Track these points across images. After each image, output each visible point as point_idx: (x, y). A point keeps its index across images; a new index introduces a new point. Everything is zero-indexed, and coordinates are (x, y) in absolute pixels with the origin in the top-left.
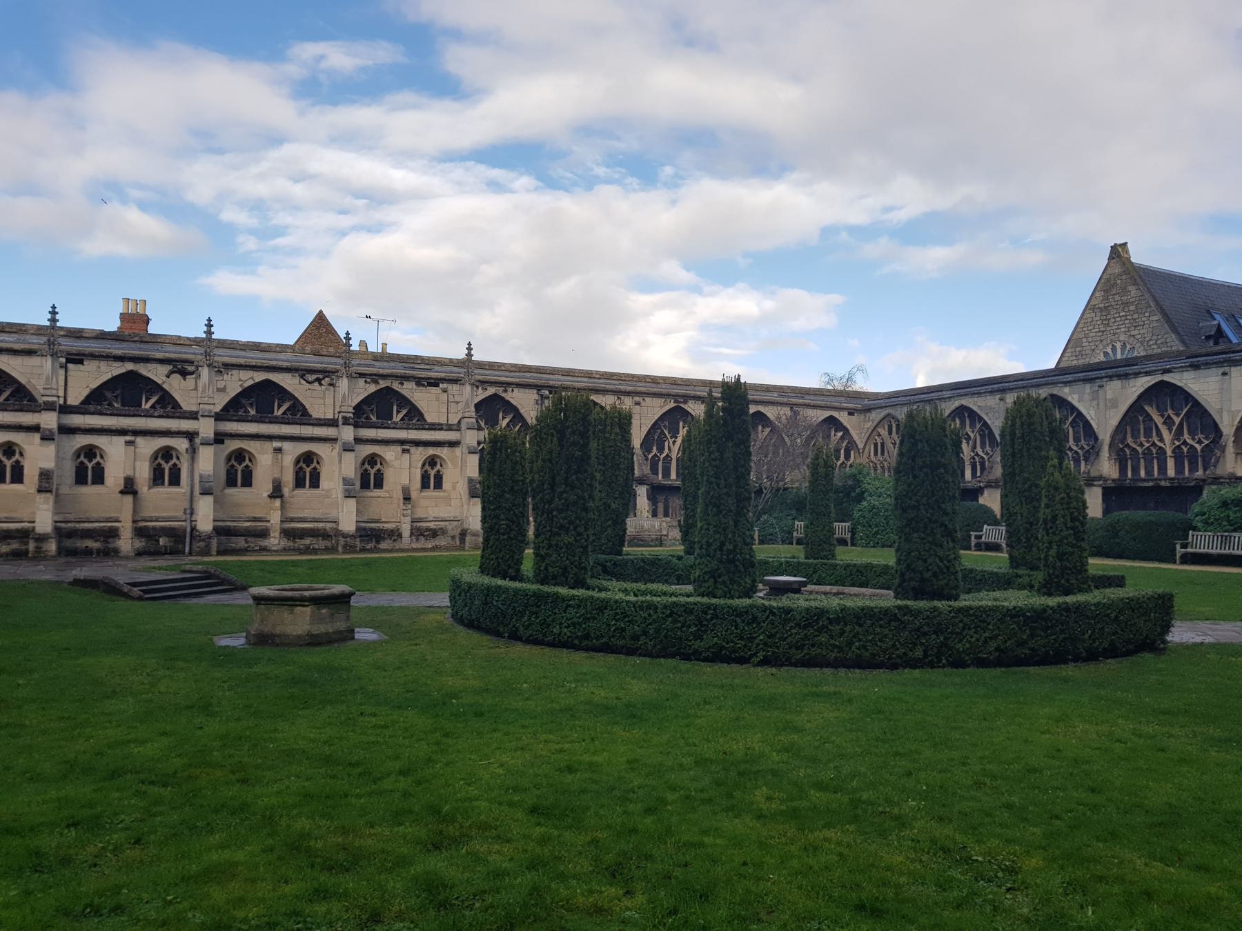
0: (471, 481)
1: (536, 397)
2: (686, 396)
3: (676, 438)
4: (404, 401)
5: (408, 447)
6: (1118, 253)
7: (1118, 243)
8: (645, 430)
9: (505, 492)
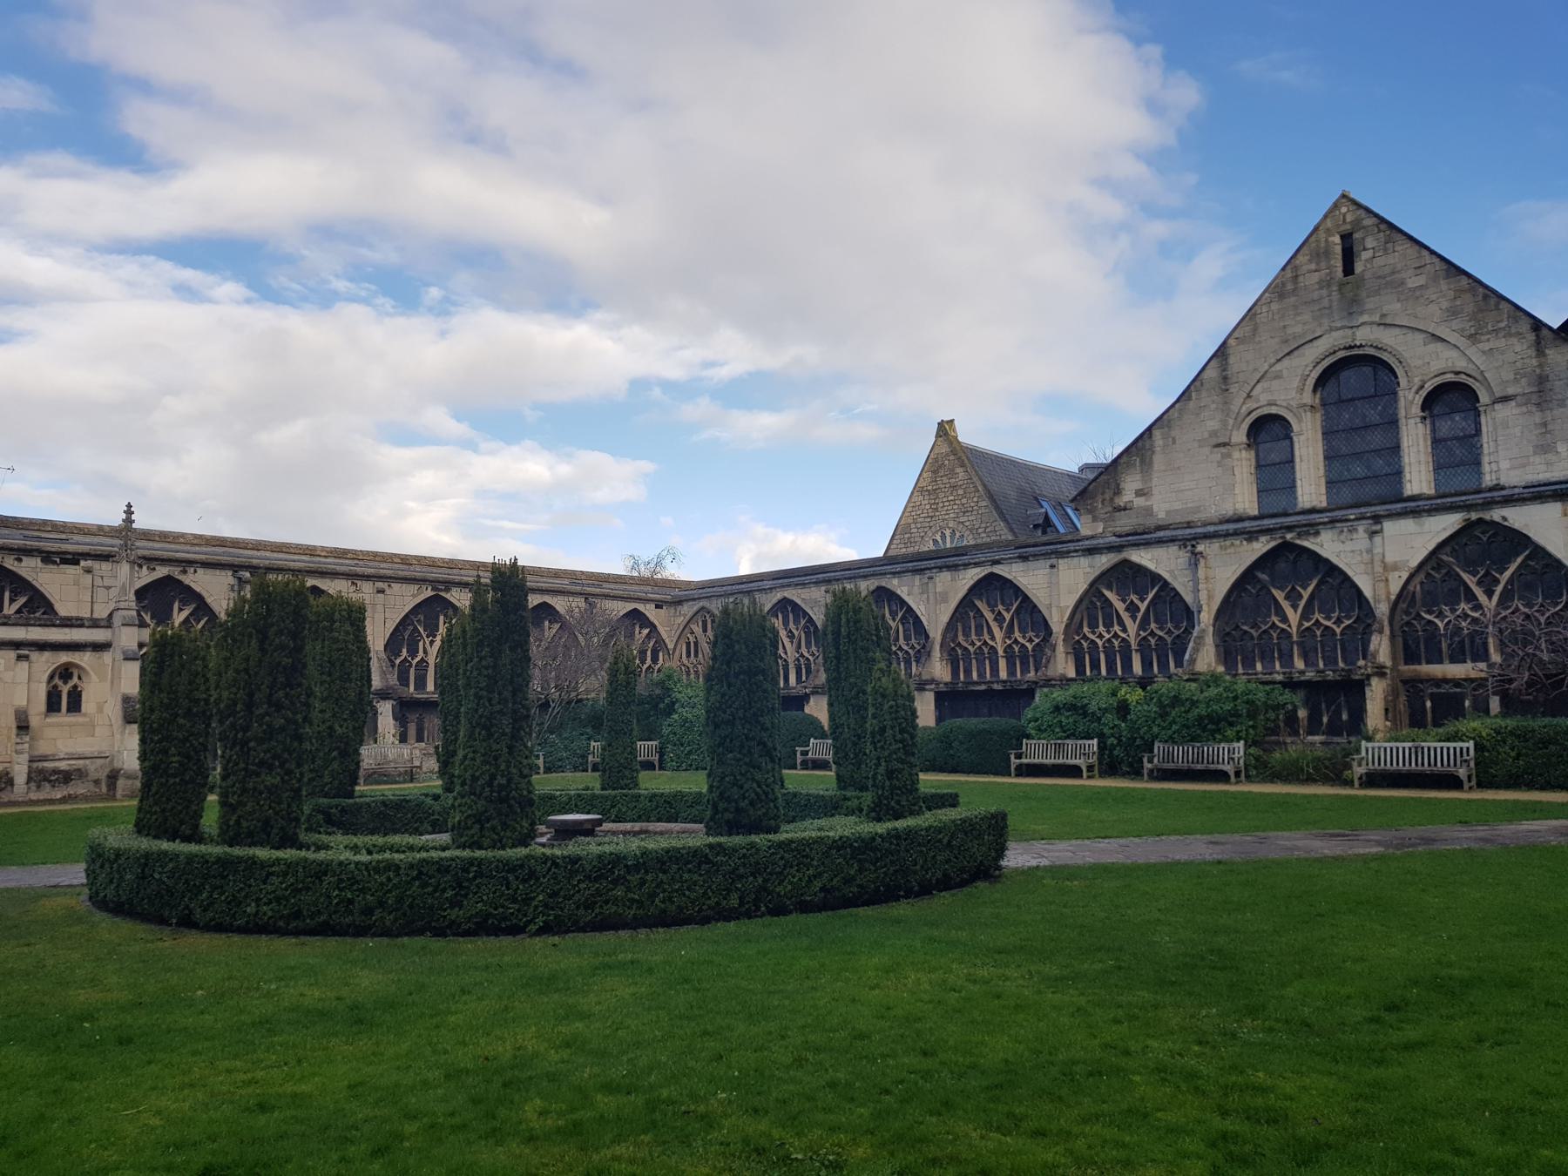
0: (126, 700)
1: (231, 580)
2: (449, 582)
3: (435, 636)
4: (21, 585)
5: (27, 652)
6: (945, 430)
7: (946, 419)
8: (391, 626)
9: (177, 715)
